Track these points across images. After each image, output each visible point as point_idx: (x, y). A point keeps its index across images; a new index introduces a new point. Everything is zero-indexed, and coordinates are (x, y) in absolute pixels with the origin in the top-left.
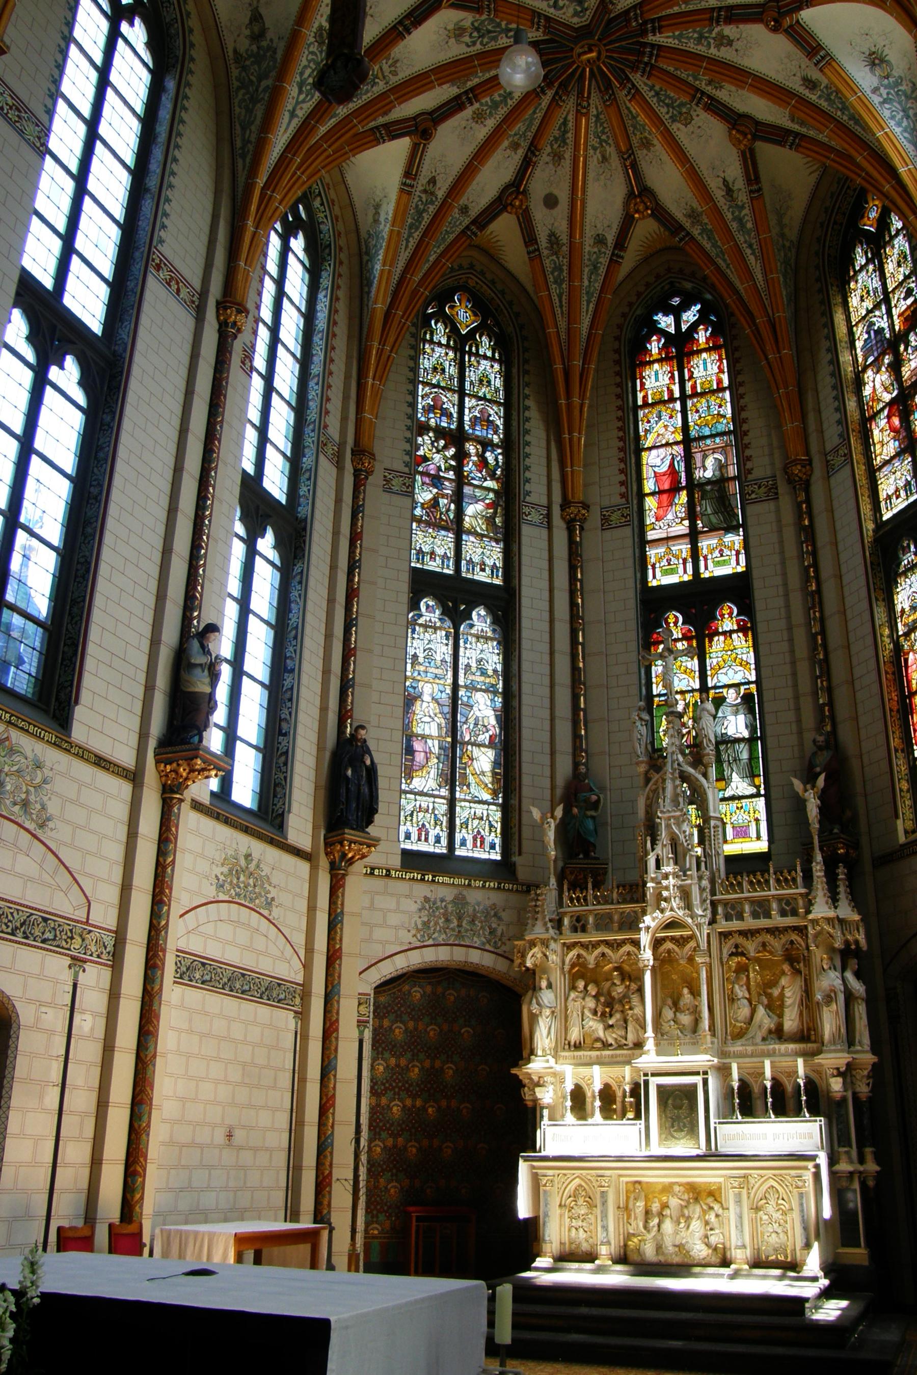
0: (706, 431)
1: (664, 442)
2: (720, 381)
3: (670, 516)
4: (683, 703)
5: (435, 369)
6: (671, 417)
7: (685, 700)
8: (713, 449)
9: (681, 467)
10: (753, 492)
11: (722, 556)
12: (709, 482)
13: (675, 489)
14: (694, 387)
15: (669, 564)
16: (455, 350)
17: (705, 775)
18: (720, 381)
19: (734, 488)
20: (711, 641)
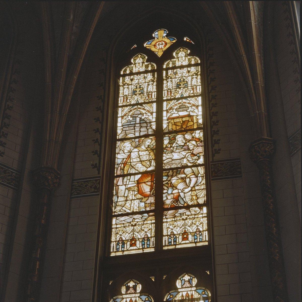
5: (134, 93)
16: (153, 71)
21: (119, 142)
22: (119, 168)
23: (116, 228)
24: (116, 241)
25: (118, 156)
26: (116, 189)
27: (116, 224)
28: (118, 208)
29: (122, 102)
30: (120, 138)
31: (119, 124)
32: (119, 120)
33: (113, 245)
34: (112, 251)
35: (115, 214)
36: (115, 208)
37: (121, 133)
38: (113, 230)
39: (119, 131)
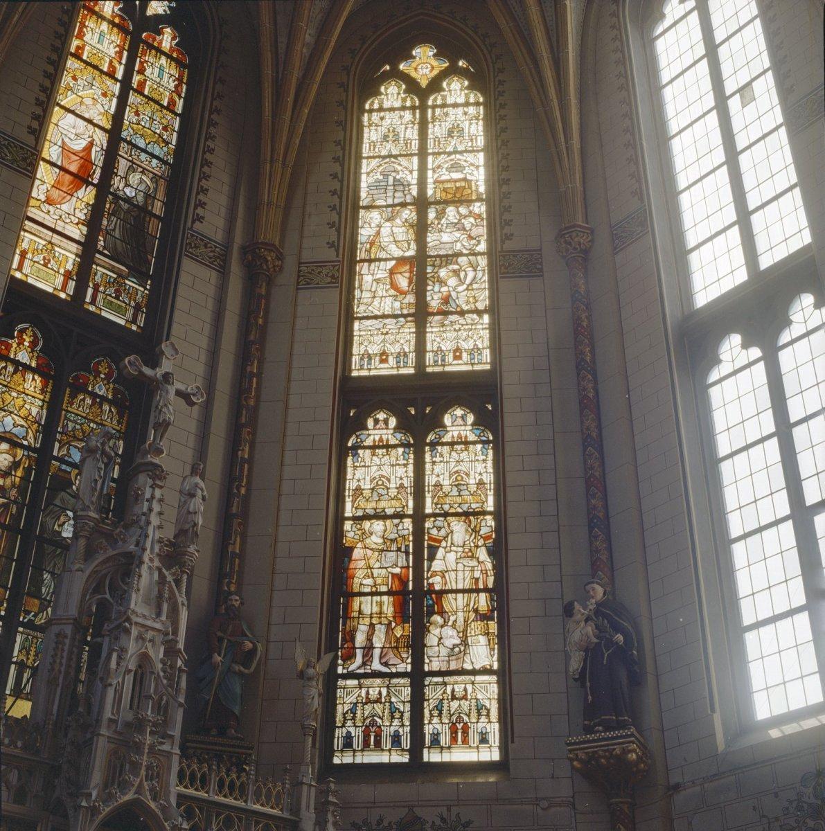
0: (141, 143)
1: (86, 115)
2: (172, 103)
3: (65, 207)
4: (11, 459)
6: (105, 95)
7: (14, 456)
8: (144, 169)
9: (97, 157)
10: (196, 247)
11: (117, 298)
12: (128, 200)
13: (81, 179)
14: (142, 84)
15: (45, 265)
17: (178, 582)
18: (172, 103)
19: (155, 228)
20: (73, 396)
21: (364, 211)
22: (364, 249)
23: (360, 336)
24: (359, 355)
25: (361, 231)
26: (359, 279)
27: (360, 330)
28: (362, 308)
29: (367, 151)
30: (364, 205)
31: (363, 185)
32: (364, 177)
33: (355, 359)
34: (353, 367)
35: (358, 315)
36: (358, 307)
37: (366, 197)
38: (355, 338)
39: (363, 195)
